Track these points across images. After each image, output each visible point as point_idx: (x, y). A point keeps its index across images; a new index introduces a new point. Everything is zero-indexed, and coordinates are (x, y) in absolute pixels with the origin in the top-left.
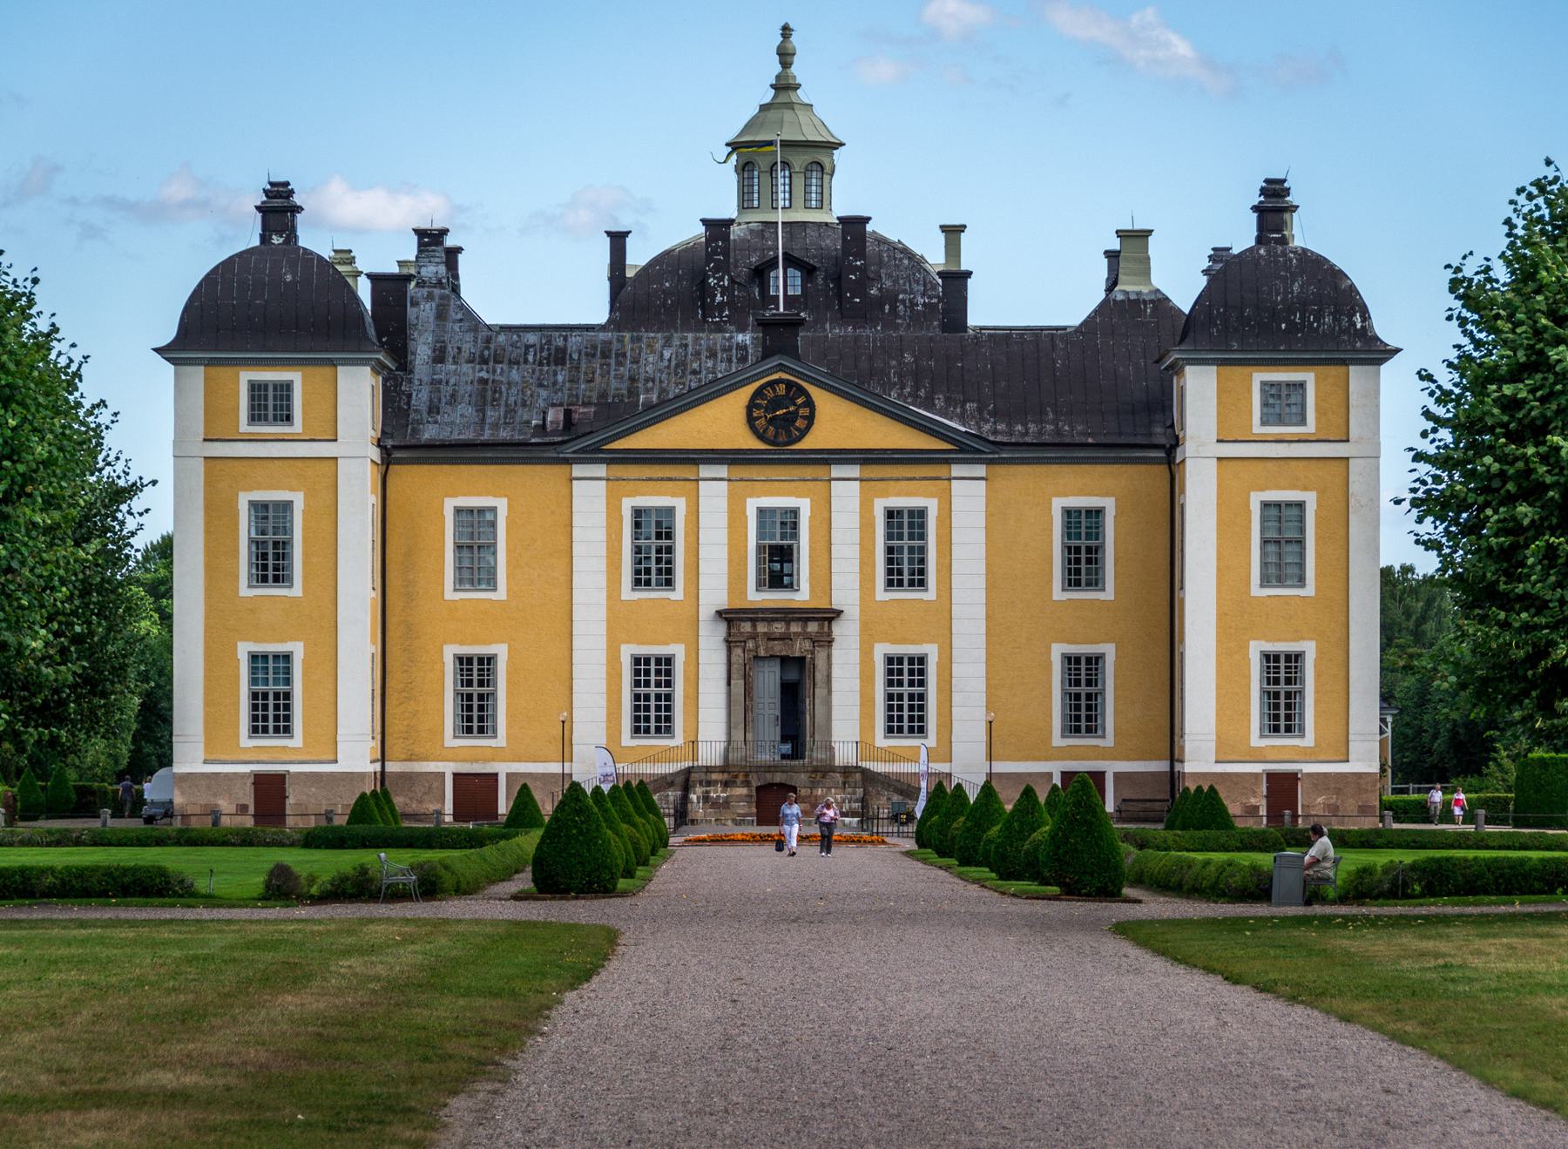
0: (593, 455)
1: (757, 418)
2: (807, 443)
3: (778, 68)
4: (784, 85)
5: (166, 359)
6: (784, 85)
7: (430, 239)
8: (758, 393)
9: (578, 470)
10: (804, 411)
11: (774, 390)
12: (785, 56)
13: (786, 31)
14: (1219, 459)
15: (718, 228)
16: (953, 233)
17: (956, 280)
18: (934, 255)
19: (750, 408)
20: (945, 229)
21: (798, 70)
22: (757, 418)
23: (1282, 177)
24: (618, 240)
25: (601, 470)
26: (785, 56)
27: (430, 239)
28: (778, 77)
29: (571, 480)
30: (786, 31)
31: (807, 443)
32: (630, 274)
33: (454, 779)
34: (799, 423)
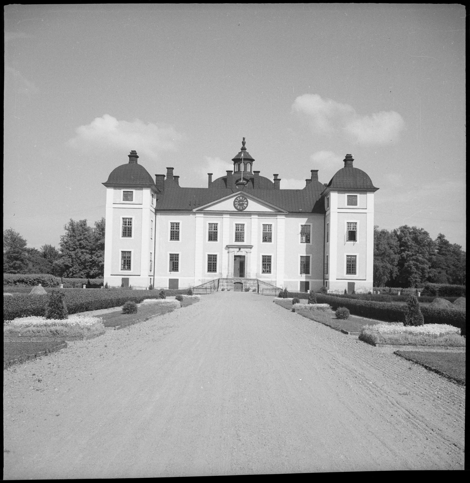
0: (200, 211)
1: (236, 204)
2: (247, 210)
3: (242, 146)
4: (243, 149)
5: (105, 186)
6: (243, 149)
7: (170, 170)
8: (236, 198)
9: (197, 215)
10: (246, 203)
11: (240, 198)
12: (244, 143)
13: (244, 139)
14: (338, 212)
15: (229, 172)
16: (276, 175)
17: (277, 180)
18: (272, 179)
19: (235, 202)
20: (274, 175)
21: (246, 146)
22: (236, 204)
23: (350, 154)
24: (210, 175)
25: (202, 215)
26: (244, 143)
27: (170, 170)
28: (242, 147)
29: (196, 217)
30: (244, 139)
31: (247, 210)
32: (213, 181)
33: (177, 279)
34: (245, 205)
